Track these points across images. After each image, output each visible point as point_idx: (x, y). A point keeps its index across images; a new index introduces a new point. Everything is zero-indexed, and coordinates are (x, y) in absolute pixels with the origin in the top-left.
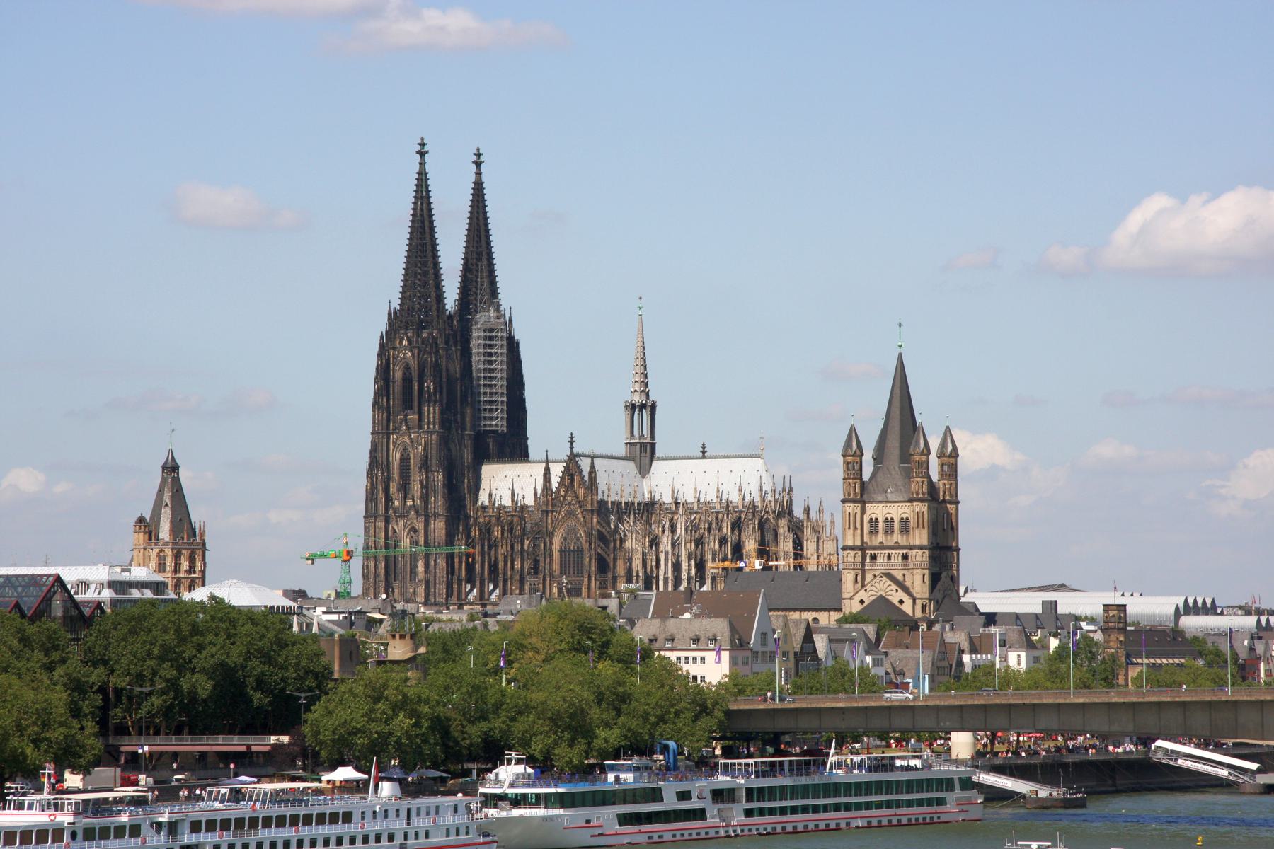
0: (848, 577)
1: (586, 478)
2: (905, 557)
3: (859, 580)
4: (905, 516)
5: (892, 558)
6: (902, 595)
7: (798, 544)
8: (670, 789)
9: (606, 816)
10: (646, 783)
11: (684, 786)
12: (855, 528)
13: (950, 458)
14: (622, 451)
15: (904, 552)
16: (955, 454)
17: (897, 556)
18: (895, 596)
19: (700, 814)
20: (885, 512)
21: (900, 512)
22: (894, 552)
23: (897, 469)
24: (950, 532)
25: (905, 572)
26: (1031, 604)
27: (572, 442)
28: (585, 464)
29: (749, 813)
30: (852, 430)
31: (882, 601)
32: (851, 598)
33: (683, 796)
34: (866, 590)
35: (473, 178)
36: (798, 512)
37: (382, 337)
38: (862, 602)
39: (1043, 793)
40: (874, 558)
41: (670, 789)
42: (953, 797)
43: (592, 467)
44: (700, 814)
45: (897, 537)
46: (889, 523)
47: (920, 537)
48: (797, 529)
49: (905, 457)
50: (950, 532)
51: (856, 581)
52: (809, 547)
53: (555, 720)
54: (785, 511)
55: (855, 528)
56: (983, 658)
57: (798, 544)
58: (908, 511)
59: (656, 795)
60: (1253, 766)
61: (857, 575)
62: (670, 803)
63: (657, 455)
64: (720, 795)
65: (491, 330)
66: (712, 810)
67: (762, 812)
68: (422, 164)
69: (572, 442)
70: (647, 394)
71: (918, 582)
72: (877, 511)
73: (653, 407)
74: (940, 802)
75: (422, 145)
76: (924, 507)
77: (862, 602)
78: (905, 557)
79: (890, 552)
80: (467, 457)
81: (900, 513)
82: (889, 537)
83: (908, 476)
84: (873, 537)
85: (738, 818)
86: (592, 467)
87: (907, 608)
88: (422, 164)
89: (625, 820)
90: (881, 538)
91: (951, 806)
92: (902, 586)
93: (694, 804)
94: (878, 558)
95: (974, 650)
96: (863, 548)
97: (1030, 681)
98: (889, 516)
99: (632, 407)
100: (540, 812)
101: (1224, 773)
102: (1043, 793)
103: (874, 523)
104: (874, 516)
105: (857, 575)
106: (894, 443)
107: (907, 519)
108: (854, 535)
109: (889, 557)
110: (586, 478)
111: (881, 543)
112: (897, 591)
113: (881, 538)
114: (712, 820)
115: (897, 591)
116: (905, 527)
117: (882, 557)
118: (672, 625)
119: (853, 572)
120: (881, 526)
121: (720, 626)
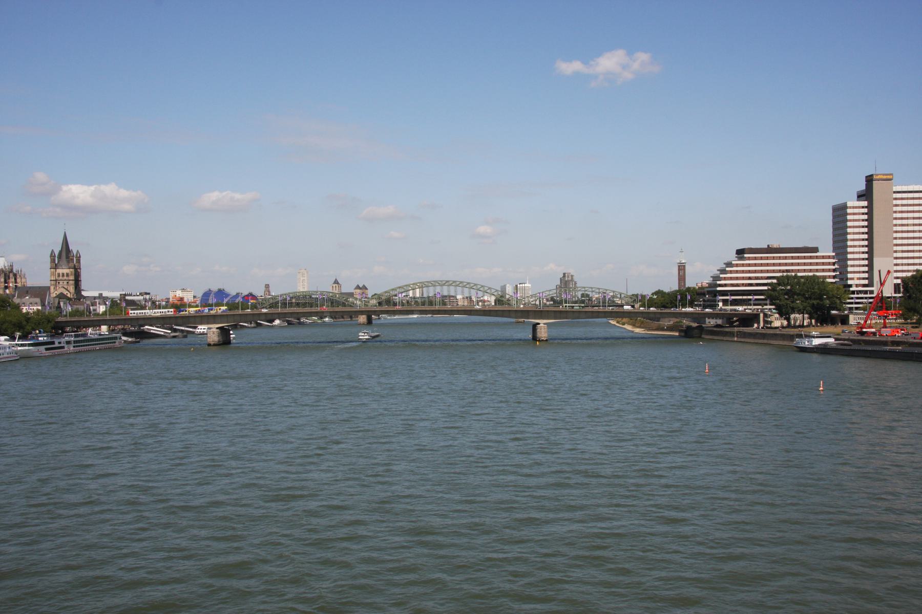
0: (52, 288)
2: (68, 283)
3: (55, 289)
6: (67, 292)
7: (16, 279)
8: (56, 341)
9: (42, 348)
10: (49, 340)
11: (59, 341)
16: (80, 257)
17: (65, 282)
18: (65, 292)
19: (63, 347)
21: (66, 271)
26: (96, 294)
29: (74, 347)
30: (53, 251)
31: (62, 294)
33: (60, 343)
36: (14, 271)
39: (130, 340)
41: (56, 341)
42: (117, 341)
44: (63, 347)
45: (65, 278)
47: (72, 278)
48: (15, 275)
49: (67, 257)
52: (18, 280)
53: (14, 325)
54: (11, 271)
56: (95, 307)
57: (16, 279)
59: (53, 343)
60: (170, 332)
62: (57, 345)
64: (68, 343)
66: (66, 346)
67: (77, 346)
71: (72, 289)
72: (60, 271)
74: (115, 342)
76: (72, 270)
83: (68, 262)
85: (72, 348)
87: (69, 295)
89: (47, 349)
90: (61, 278)
91: (117, 344)
92: (67, 290)
93: (62, 345)
95: (92, 306)
96: (56, 280)
97: (105, 313)
100: (27, 348)
101: (163, 333)
102: (130, 340)
106: (64, 254)
113: (61, 278)
114: (66, 349)
116: (68, 275)
117: (61, 282)
118: (23, 300)
120: (61, 275)
121: (38, 300)
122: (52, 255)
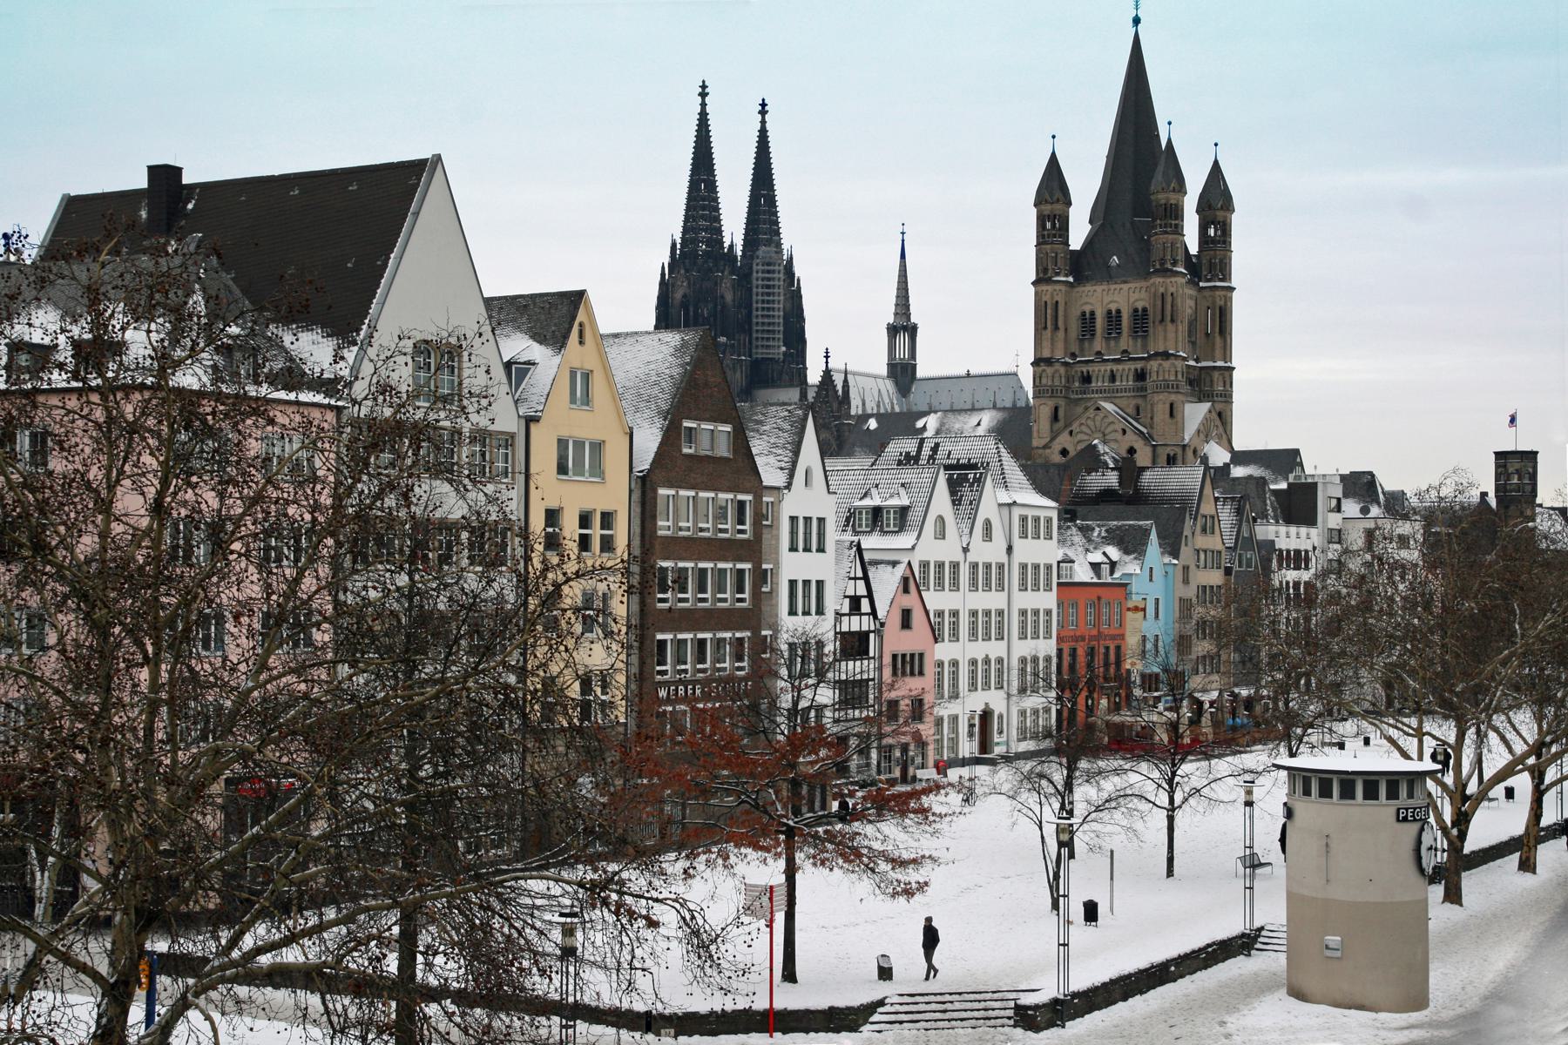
1: (840, 393)
2: (1141, 376)
4: (1140, 305)
5: (1118, 378)
12: (1056, 328)
13: (1217, 201)
14: (884, 371)
15: (1139, 365)
20: (1106, 299)
22: (1120, 367)
23: (1128, 225)
24: (1218, 340)
25: (1140, 401)
27: (827, 357)
28: (838, 380)
32: (1046, 447)
34: (1071, 433)
35: (758, 126)
37: (663, 268)
38: (1064, 452)
40: (1087, 379)
43: (846, 381)
45: (1125, 342)
46: (1113, 318)
50: (1218, 340)
51: (1055, 418)
55: (1056, 328)
58: (1144, 295)
61: (1056, 409)
63: (920, 374)
65: (769, 264)
68: (703, 105)
69: (827, 357)
70: (908, 316)
73: (912, 330)
75: (704, 87)
77: (1064, 452)
78: (1141, 376)
79: (1115, 367)
80: (738, 378)
81: (1132, 300)
82: (1112, 343)
84: (1086, 344)
86: (846, 381)
88: (703, 105)
94: (1094, 379)
98: (1113, 307)
99: (893, 331)
103: (1088, 321)
104: (1087, 309)
105: (1056, 409)
107: (1145, 310)
108: (1052, 339)
109: (1113, 378)
110: (840, 393)
111: (1099, 353)
112: (1124, 432)
115: (1124, 432)
119: (1051, 403)
122: (1053, 189)
